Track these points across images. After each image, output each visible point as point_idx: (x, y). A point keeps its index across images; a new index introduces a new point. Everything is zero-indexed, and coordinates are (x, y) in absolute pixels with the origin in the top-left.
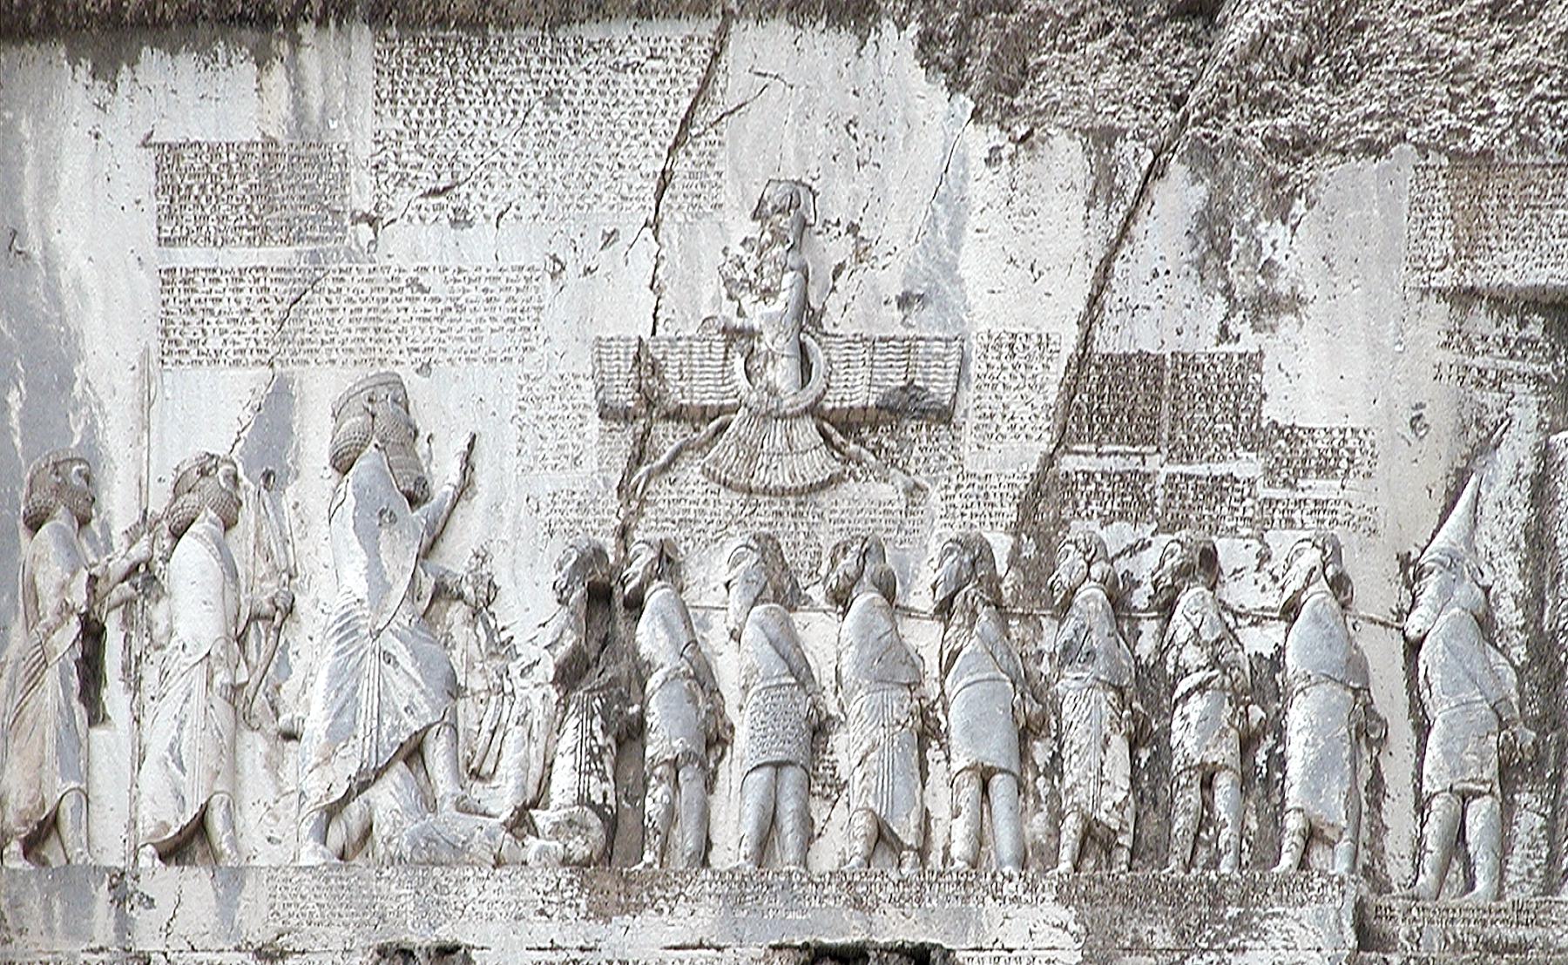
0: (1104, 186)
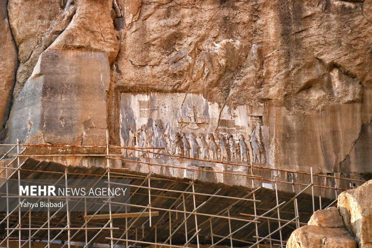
0: (220, 107)
